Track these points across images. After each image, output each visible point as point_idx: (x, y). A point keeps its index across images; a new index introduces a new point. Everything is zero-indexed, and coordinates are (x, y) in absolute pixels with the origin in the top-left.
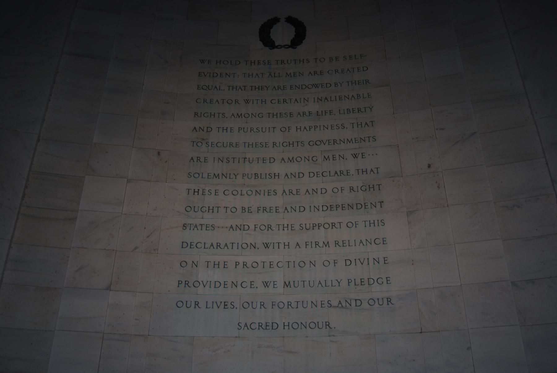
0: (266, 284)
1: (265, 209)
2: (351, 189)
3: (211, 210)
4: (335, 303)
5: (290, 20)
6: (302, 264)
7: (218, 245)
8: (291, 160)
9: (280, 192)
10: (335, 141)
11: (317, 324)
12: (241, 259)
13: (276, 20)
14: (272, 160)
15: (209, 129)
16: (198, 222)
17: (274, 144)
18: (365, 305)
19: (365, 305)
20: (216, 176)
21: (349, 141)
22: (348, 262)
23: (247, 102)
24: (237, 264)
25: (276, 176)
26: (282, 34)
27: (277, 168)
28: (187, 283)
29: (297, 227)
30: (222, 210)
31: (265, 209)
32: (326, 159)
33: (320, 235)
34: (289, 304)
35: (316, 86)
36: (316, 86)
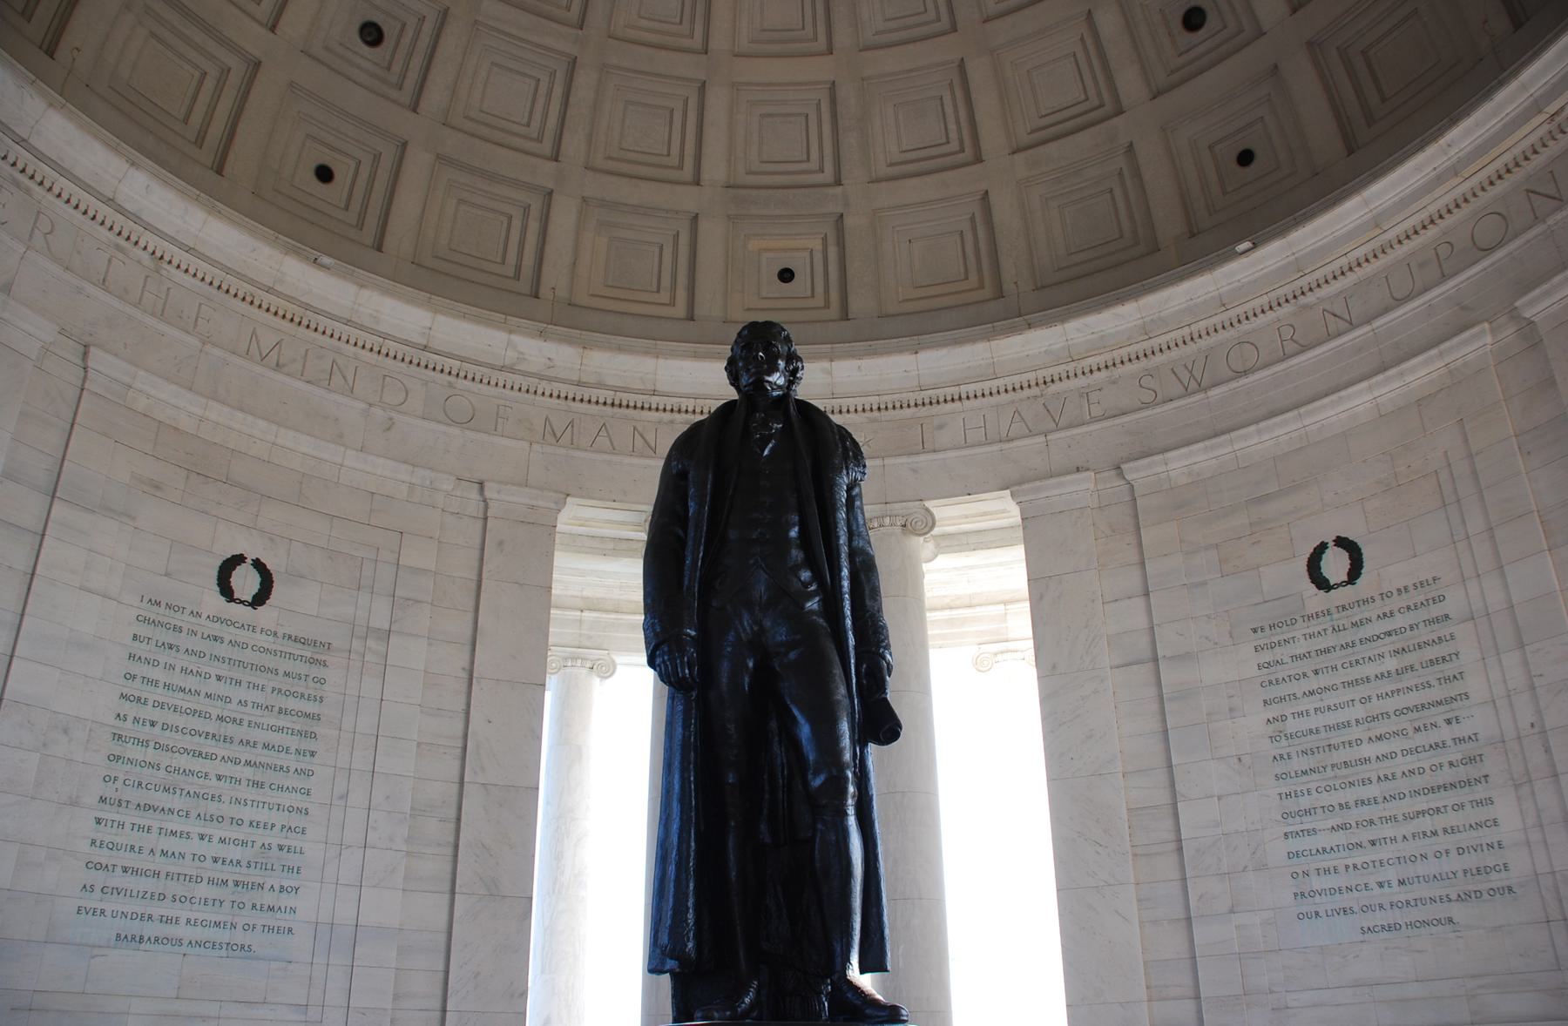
0: (1381, 885)
1: (1363, 802)
2: (1451, 764)
3: (1307, 812)
4: (1454, 897)
5: (1341, 542)
6: (1413, 859)
7: (1324, 850)
8: (1379, 738)
9: (1375, 779)
10: (1423, 706)
11: (1439, 921)
12: (1350, 862)
13: (1322, 547)
14: (1359, 742)
15: (1283, 718)
16: (1298, 828)
17: (1357, 721)
18: (1486, 896)
19: (1486, 896)
20: (1304, 773)
21: (1440, 703)
22: (1461, 851)
23: (1316, 672)
24: (1347, 867)
25: (1367, 760)
26: (1335, 565)
27: (1369, 750)
28: (1303, 894)
29: (1400, 818)
30: (1319, 811)
31: (1363, 802)
32: (1417, 730)
33: (1426, 823)
34: (1408, 903)
35: (1389, 634)
36: (1389, 634)
